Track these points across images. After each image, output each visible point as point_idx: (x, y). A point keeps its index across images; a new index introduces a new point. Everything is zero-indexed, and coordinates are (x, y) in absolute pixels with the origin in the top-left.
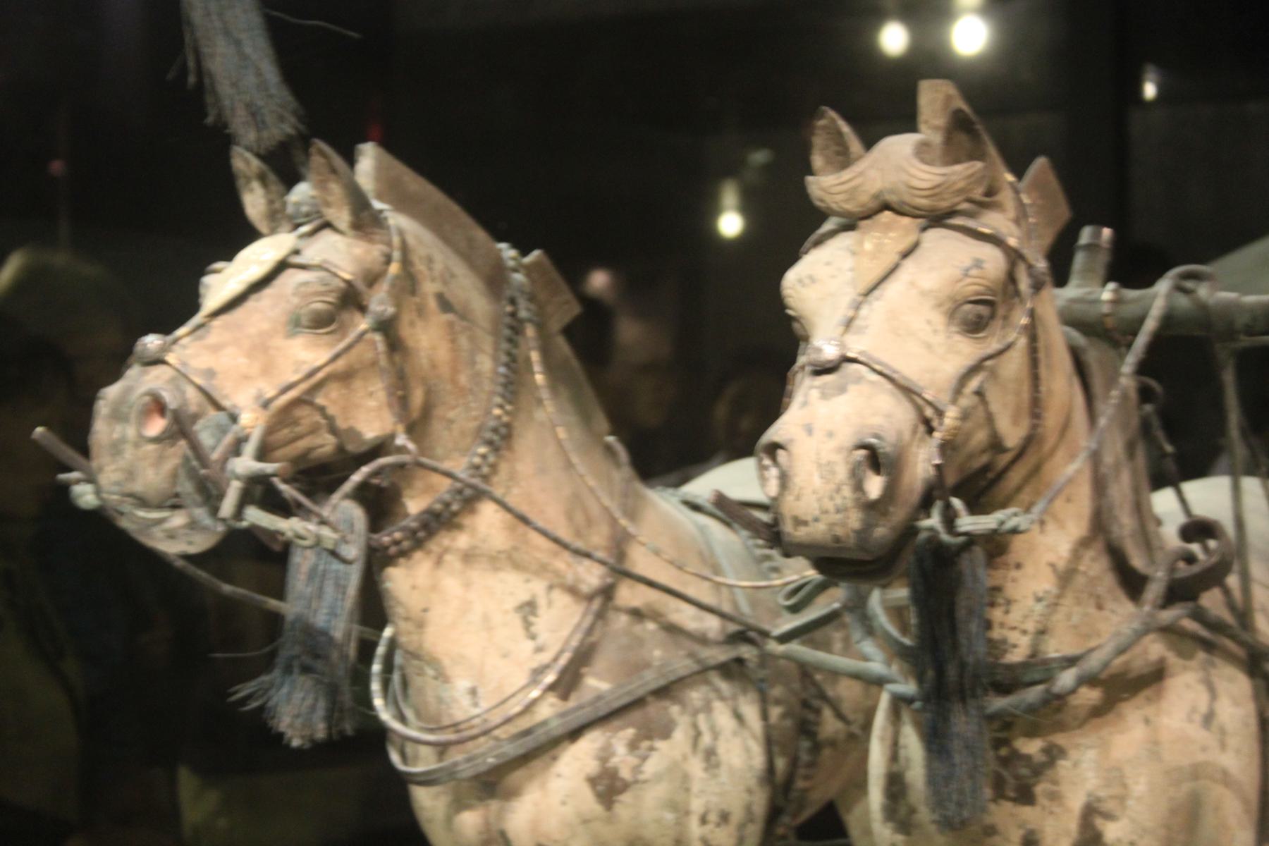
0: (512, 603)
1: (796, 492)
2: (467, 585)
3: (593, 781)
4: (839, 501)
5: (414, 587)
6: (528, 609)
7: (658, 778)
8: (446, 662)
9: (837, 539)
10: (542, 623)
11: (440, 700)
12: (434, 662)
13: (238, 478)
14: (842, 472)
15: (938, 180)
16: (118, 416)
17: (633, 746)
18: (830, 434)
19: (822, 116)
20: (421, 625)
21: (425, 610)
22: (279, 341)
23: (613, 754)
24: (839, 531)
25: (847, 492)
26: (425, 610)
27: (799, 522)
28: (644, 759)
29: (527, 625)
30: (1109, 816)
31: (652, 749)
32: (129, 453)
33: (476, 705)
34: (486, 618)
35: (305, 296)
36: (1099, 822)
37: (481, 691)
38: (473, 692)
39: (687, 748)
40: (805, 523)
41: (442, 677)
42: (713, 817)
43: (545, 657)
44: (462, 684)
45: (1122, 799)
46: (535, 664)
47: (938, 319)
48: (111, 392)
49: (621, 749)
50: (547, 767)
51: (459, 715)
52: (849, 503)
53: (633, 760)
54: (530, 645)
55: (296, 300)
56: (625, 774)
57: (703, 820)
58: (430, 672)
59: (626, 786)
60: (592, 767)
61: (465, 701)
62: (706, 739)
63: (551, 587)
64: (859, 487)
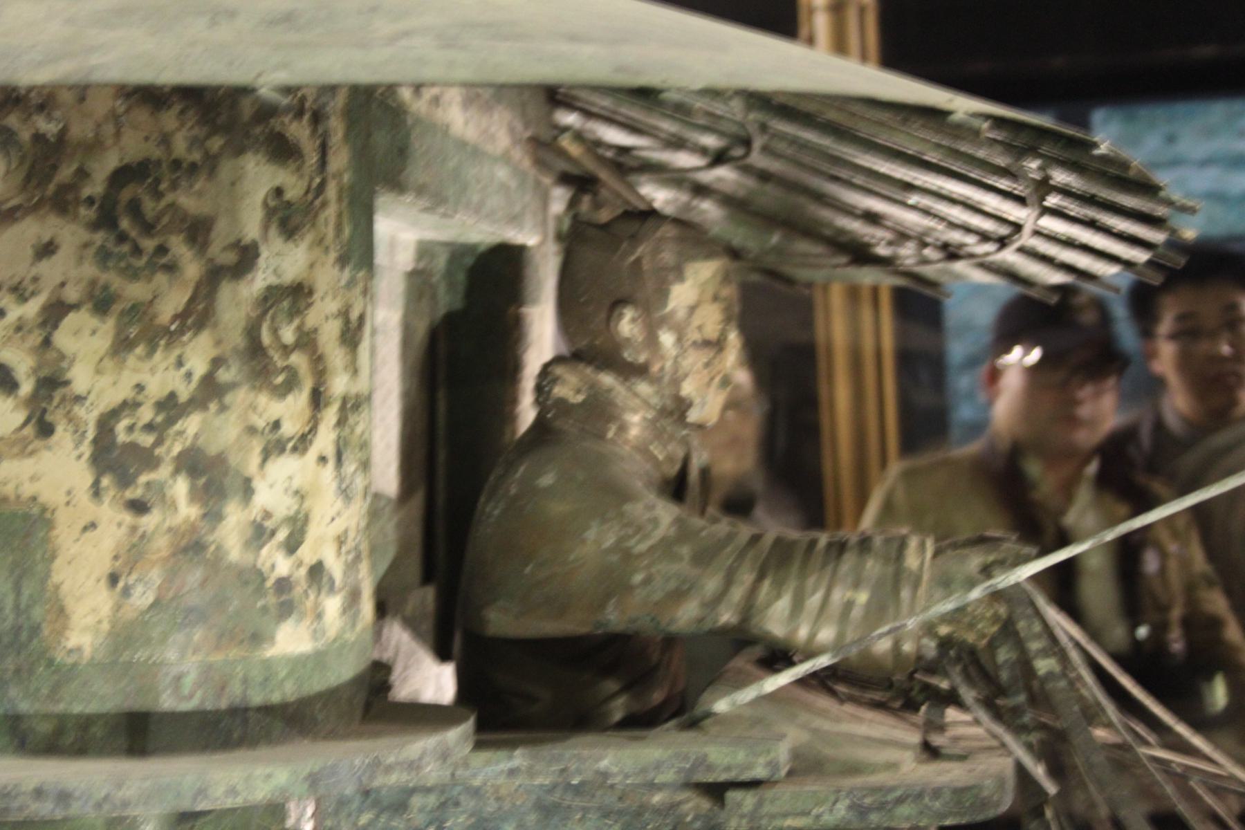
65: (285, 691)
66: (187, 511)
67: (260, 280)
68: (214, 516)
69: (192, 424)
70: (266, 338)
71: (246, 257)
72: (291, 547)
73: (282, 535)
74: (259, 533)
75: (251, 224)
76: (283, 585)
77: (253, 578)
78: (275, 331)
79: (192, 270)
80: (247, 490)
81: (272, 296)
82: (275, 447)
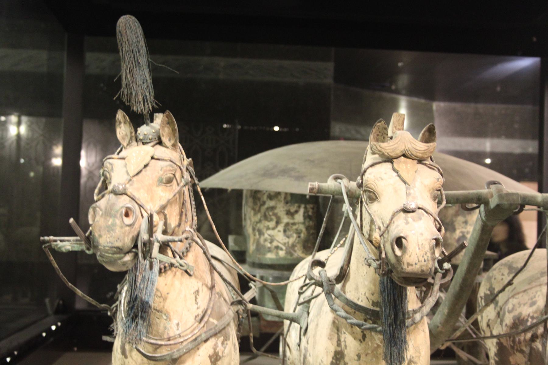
1: (409, 254)
2: (181, 284)
3: (210, 357)
4: (426, 257)
5: (166, 285)
8: (171, 314)
9: (423, 271)
11: (165, 328)
12: (167, 314)
13: (158, 242)
14: (427, 248)
15: (426, 148)
16: (108, 213)
18: (422, 234)
19: (380, 122)
20: (165, 299)
21: (168, 294)
22: (155, 188)
23: (218, 347)
24: (424, 268)
25: (429, 254)
26: (168, 294)
27: (408, 264)
28: (225, 348)
32: (118, 230)
33: (178, 329)
35: (165, 171)
37: (180, 324)
38: (178, 325)
40: (412, 265)
41: (169, 319)
44: (175, 321)
45: (419, 357)
47: (429, 195)
49: (220, 344)
50: (195, 352)
51: (171, 334)
52: (430, 259)
53: (222, 348)
54: (196, 306)
55: (161, 173)
56: (220, 354)
58: (165, 317)
60: (211, 352)
61: (175, 328)
63: (203, 285)
64: (434, 253)
65: (269, 262)
66: (257, 236)
67: (266, 206)
68: (260, 237)
69: (258, 225)
70: (267, 214)
71: (264, 203)
72: (271, 243)
73: (269, 241)
74: (265, 240)
75: (265, 198)
76: (269, 248)
77: (264, 246)
78: (268, 213)
79: (259, 204)
80: (263, 234)
81: (268, 209)
82: (268, 228)
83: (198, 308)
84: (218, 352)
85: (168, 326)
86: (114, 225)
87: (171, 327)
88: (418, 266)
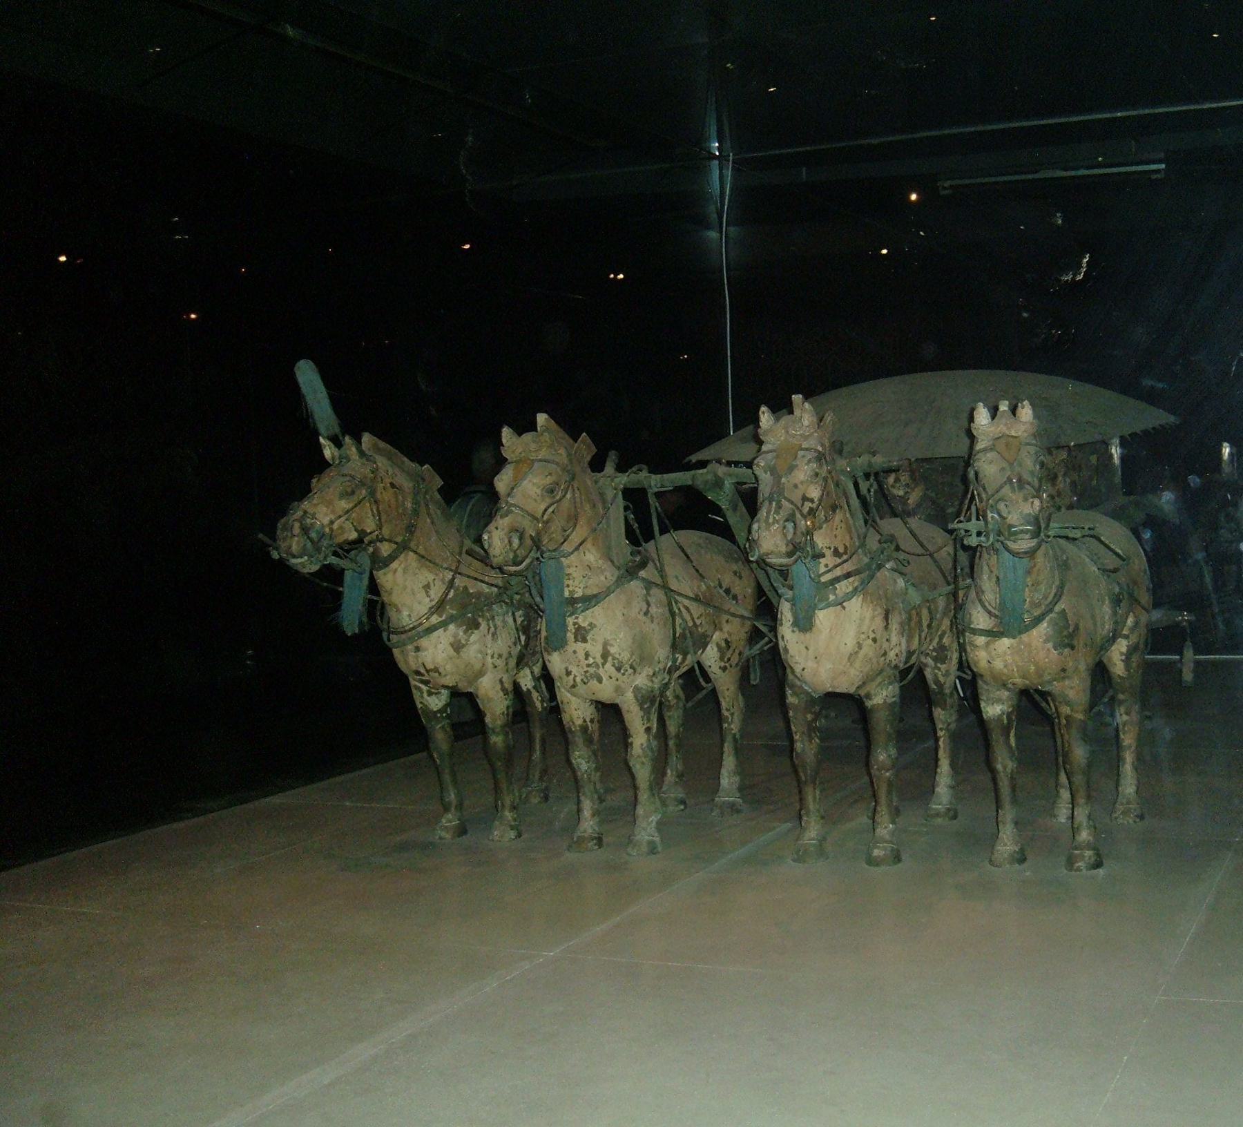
0: (421, 586)
3: (452, 645)
6: (427, 587)
7: (475, 643)
8: (400, 606)
10: (432, 593)
12: (396, 606)
17: (465, 632)
20: (390, 594)
29: (427, 592)
30: (612, 645)
31: (473, 633)
34: (412, 590)
36: (609, 647)
38: (409, 616)
39: (486, 631)
40: (497, 557)
42: (496, 656)
43: (434, 603)
44: (405, 613)
46: (430, 606)
48: (283, 521)
56: (463, 642)
57: (492, 657)
59: (464, 646)
62: (492, 629)
83: (431, 601)
84: (460, 640)
85: (400, 618)
86: (287, 536)
87: (403, 618)
88: (501, 558)
